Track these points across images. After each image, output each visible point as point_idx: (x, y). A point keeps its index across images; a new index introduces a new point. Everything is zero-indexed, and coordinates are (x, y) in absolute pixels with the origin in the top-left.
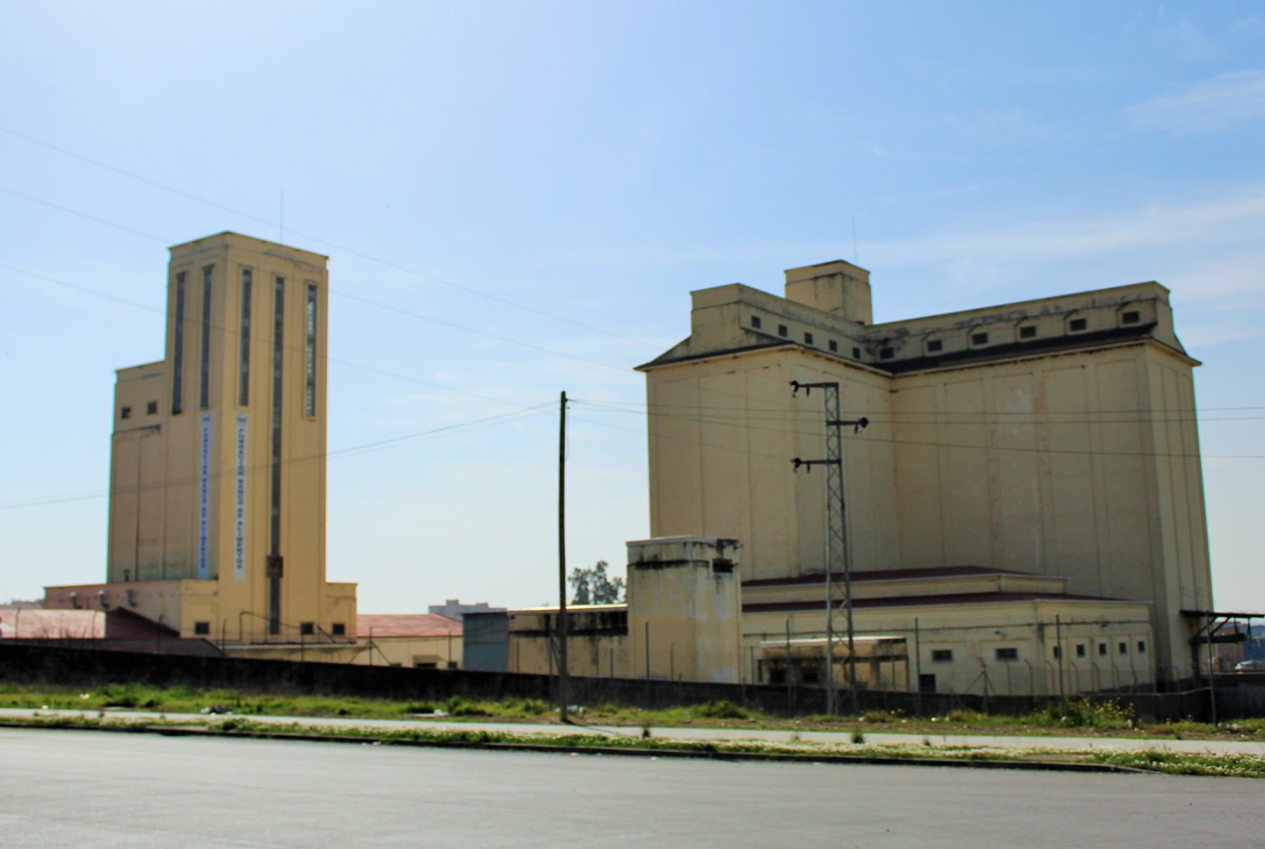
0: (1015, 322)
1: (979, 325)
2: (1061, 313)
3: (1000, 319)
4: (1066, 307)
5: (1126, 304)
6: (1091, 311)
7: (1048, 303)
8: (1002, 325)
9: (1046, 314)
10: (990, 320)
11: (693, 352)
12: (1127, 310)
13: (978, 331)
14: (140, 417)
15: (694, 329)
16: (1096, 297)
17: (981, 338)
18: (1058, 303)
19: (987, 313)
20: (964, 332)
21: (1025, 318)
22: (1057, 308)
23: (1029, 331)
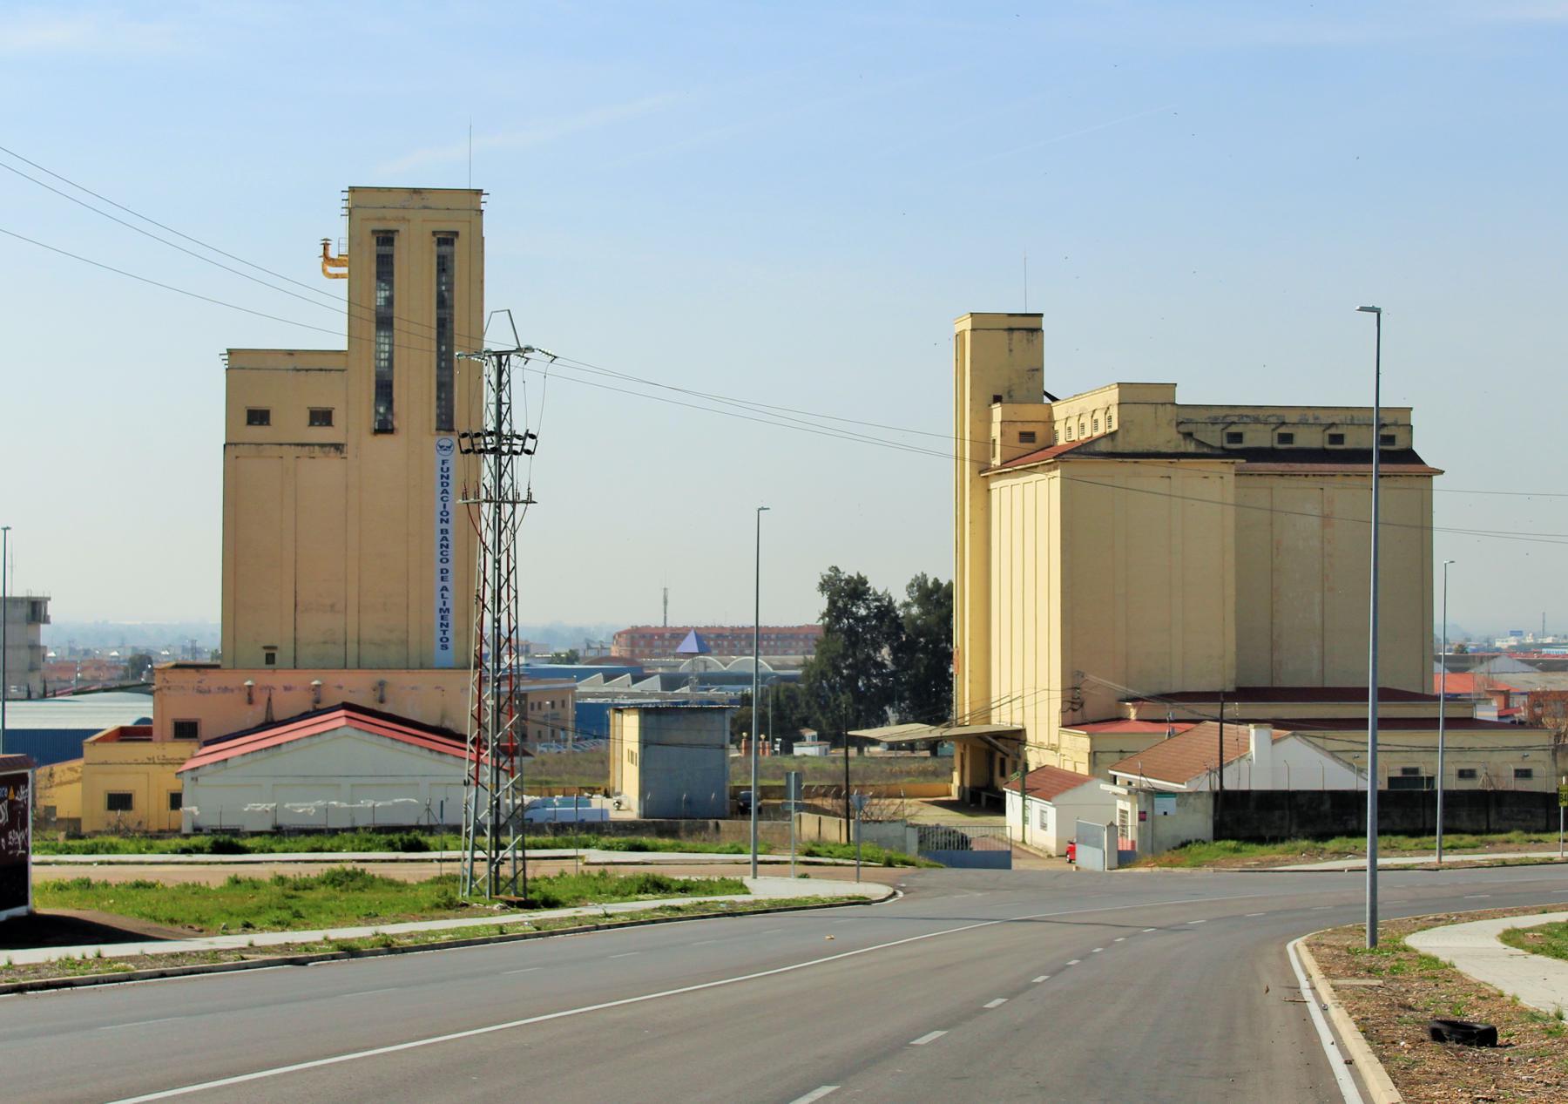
0: (1273, 426)
1: (1233, 423)
2: (1321, 425)
3: (1257, 421)
4: (1326, 419)
6: (1350, 427)
7: (1307, 412)
8: (1260, 427)
9: (1303, 423)
10: (1245, 419)
11: (1119, 449)
13: (1234, 429)
16: (1355, 414)
18: (1317, 413)
19: (1245, 412)
20: (1219, 427)
21: (1283, 423)
22: (1317, 418)
23: (1287, 438)
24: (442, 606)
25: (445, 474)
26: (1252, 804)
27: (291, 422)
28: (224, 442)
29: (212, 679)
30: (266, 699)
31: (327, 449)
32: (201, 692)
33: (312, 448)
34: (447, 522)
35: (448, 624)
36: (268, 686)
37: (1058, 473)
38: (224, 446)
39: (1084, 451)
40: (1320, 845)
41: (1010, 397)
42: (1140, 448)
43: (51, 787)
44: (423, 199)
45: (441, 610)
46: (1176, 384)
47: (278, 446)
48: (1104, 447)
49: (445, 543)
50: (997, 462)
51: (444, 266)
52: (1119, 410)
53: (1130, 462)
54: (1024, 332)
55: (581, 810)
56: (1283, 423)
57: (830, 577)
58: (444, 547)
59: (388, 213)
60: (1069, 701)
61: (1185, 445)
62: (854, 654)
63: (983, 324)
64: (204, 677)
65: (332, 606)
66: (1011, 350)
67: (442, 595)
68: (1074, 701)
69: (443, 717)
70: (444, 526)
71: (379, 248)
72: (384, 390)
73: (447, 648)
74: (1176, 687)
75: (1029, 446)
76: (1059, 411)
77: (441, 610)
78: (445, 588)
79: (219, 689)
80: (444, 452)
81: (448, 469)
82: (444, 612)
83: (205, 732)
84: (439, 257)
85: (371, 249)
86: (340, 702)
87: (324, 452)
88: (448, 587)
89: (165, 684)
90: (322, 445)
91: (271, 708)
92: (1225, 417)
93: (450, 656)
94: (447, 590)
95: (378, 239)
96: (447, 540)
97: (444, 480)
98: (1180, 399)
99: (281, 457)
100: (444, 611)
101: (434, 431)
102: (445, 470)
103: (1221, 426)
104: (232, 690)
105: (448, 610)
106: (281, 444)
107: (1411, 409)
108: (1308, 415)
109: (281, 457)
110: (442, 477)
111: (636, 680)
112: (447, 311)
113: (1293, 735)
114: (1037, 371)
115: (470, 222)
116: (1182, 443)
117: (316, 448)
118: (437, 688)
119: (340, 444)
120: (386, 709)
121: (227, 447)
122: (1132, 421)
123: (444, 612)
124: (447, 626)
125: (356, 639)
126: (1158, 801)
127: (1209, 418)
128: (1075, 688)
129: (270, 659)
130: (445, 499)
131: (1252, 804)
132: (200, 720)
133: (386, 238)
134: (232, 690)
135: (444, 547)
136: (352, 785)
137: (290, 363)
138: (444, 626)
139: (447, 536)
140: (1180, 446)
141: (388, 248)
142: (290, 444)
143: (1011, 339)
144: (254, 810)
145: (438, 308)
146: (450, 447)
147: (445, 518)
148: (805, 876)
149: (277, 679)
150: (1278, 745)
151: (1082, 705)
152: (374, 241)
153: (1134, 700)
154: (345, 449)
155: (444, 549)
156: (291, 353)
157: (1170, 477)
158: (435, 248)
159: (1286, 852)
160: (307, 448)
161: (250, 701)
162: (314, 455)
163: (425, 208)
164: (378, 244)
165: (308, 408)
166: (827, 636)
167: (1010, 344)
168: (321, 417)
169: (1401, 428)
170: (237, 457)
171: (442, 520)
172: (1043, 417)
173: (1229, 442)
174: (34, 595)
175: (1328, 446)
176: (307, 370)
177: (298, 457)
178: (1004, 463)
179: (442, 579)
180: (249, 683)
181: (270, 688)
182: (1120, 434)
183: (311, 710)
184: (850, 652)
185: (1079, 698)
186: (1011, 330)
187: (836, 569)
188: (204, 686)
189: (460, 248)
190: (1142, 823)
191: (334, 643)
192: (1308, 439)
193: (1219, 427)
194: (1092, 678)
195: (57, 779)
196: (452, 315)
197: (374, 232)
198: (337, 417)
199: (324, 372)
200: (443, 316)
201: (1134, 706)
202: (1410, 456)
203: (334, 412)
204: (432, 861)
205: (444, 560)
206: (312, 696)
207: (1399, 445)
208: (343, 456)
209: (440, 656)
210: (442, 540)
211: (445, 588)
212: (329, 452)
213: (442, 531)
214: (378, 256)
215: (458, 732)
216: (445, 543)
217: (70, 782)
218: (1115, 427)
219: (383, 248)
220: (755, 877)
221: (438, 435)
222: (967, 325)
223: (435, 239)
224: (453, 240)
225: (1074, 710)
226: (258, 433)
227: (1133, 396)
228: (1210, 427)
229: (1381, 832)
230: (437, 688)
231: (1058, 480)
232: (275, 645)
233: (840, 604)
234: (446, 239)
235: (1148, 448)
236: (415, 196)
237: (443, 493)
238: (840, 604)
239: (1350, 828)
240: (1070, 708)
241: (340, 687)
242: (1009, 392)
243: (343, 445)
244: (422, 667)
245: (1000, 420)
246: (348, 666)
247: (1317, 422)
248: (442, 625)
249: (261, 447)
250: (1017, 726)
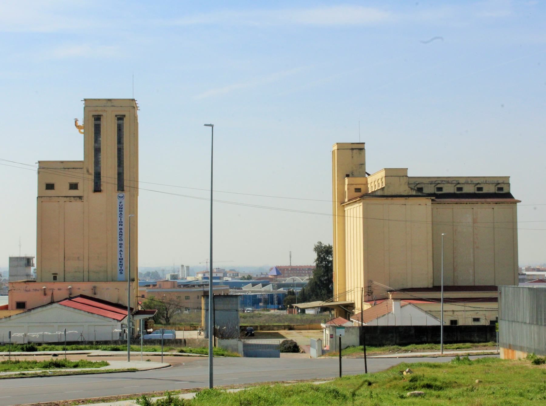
0: (455, 185)
1: (439, 183)
2: (474, 184)
3: (448, 182)
4: (475, 181)
5: (499, 184)
7: (467, 179)
9: (467, 183)
10: (444, 182)
11: (386, 194)
12: (499, 186)
13: (439, 186)
17: (440, 189)
18: (472, 179)
19: (443, 179)
21: (459, 183)
22: (472, 181)
23: (460, 189)
24: (120, 257)
25: (121, 207)
26: (379, 331)
27: (62, 188)
28: (37, 196)
29: (31, 286)
30: (51, 293)
31: (76, 198)
32: (26, 291)
33: (70, 198)
34: (122, 225)
35: (122, 264)
36: (52, 289)
37: (361, 204)
38: (37, 197)
39: (374, 195)
40: (400, 347)
41: (353, 175)
42: (393, 194)
44: (112, 103)
45: (120, 259)
46: (407, 169)
48: (380, 193)
49: (121, 233)
50: (346, 200)
51: (120, 129)
52: (385, 178)
54: (358, 150)
55: (69, 334)
56: (459, 183)
57: (318, 246)
58: (121, 235)
59: (99, 109)
60: (367, 292)
61: (412, 192)
62: (328, 275)
63: (341, 147)
64: (27, 285)
65: (78, 258)
66: (352, 157)
67: (120, 253)
68: (369, 292)
69: (118, 300)
70: (121, 227)
71: (95, 122)
72: (98, 175)
73: (122, 273)
74: (409, 286)
75: (359, 194)
76: (370, 179)
77: (120, 259)
78: (121, 251)
79: (33, 289)
80: (120, 199)
81: (122, 205)
82: (121, 260)
83: (28, 306)
84: (118, 125)
85: (92, 122)
86: (79, 294)
87: (75, 200)
88: (122, 250)
89: (13, 288)
90: (74, 197)
91: (53, 297)
92: (435, 181)
93: (122, 277)
94: (122, 251)
95: (95, 118)
96: (122, 232)
97: (121, 209)
98: (409, 175)
99: (59, 202)
100: (121, 259)
101: (117, 191)
102: (121, 205)
103: (434, 185)
104: (38, 290)
105: (122, 259)
106: (58, 197)
107: (509, 177)
108: (469, 180)
109: (59, 202)
110: (120, 208)
111: (264, 286)
112: (121, 145)
113: (410, 303)
114: (363, 165)
115: (130, 111)
116: (410, 191)
117: (72, 198)
118: (116, 289)
119: (81, 196)
120: (97, 297)
121: (38, 198)
122: (391, 183)
123: (121, 260)
124: (122, 265)
125: (87, 270)
126: (337, 330)
127: (429, 182)
128: (369, 287)
129: (55, 278)
130: (121, 217)
131: (379, 331)
132: (26, 302)
133: (98, 118)
134: (38, 290)
135: (121, 235)
136: (59, 326)
137: (62, 166)
138: (121, 265)
139: (122, 231)
140: (409, 192)
141: (98, 122)
142: (62, 197)
143: (352, 153)
144: (35, 336)
145: (118, 144)
146: (122, 197)
147: (121, 224)
148: (148, 360)
149: (56, 286)
150: (403, 308)
151: (372, 293)
152: (93, 119)
153: (391, 291)
154: (83, 199)
155: (121, 236)
156: (62, 162)
157: (405, 205)
158: (116, 121)
159: (384, 350)
160: (68, 198)
161: (45, 294)
162: (71, 201)
163: (113, 106)
164: (95, 120)
165: (69, 183)
166: (317, 268)
167: (352, 154)
168: (74, 186)
169: (506, 184)
170: (42, 202)
171: (120, 225)
172: (364, 182)
173: (437, 191)
174: (28, 256)
175: (497, 192)
176: (68, 168)
177: (65, 201)
178: (349, 200)
179: (120, 247)
180: (44, 287)
181: (53, 289)
182: (386, 188)
184: (326, 274)
185: (370, 291)
186: (352, 149)
187: (321, 243)
188: (28, 289)
189: (126, 122)
190: (331, 339)
191: (79, 272)
192: (449, 189)
193: (453, 185)
194: (375, 283)
196: (123, 147)
197: (93, 116)
198: (80, 186)
199: (75, 169)
200: (119, 147)
201: (391, 294)
202: (509, 195)
203: (78, 184)
204: (33, 355)
205: (121, 240)
206: (68, 292)
207: (505, 191)
208: (82, 201)
209: (119, 276)
210: (120, 232)
211: (121, 251)
212: (77, 199)
213: (120, 229)
214: (95, 125)
215: (124, 306)
216: (121, 233)
218: (384, 186)
219: (97, 122)
220: (129, 361)
221: (118, 192)
222: (336, 148)
223: (116, 118)
224: (123, 118)
225: (369, 295)
226: (50, 192)
227: (391, 174)
228: (430, 185)
229: (445, 343)
230: (116, 289)
231: (361, 207)
232: (57, 273)
233: (322, 256)
234: (121, 118)
235: (397, 193)
237: (120, 214)
238: (322, 256)
239: (423, 340)
240: (367, 295)
241: (79, 289)
242: (352, 173)
243: (82, 197)
244: (113, 280)
245: (347, 184)
246: (84, 281)
247: (472, 183)
248: (120, 265)
249: (51, 198)
250: (353, 302)
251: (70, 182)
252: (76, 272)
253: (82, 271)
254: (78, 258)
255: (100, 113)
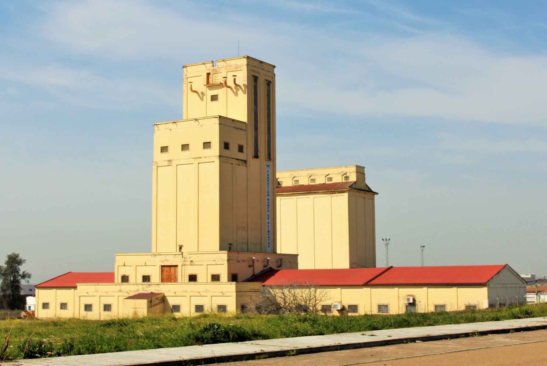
11: (357, 187)
14: (233, 151)
15: (357, 179)
31: (243, 162)
43: (151, 307)
47: (231, 159)
53: (355, 191)
65: (244, 227)
78: (269, 223)
99: (232, 164)
101: (267, 159)
117: (241, 161)
156: (233, 120)
162: (240, 164)
165: (238, 144)
183: (263, 270)
195: (153, 304)
211: (269, 223)
217: (156, 305)
236: (261, 64)
251: (239, 144)
252: (243, 243)
253: (247, 242)
254: (244, 227)
255: (257, 75)
